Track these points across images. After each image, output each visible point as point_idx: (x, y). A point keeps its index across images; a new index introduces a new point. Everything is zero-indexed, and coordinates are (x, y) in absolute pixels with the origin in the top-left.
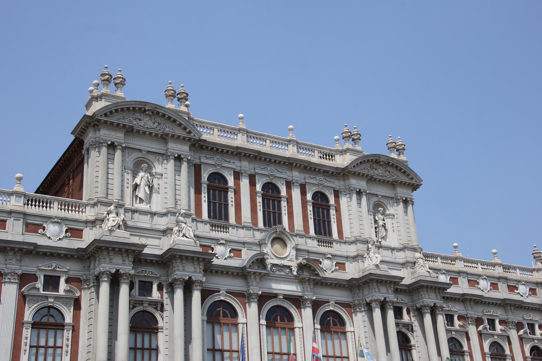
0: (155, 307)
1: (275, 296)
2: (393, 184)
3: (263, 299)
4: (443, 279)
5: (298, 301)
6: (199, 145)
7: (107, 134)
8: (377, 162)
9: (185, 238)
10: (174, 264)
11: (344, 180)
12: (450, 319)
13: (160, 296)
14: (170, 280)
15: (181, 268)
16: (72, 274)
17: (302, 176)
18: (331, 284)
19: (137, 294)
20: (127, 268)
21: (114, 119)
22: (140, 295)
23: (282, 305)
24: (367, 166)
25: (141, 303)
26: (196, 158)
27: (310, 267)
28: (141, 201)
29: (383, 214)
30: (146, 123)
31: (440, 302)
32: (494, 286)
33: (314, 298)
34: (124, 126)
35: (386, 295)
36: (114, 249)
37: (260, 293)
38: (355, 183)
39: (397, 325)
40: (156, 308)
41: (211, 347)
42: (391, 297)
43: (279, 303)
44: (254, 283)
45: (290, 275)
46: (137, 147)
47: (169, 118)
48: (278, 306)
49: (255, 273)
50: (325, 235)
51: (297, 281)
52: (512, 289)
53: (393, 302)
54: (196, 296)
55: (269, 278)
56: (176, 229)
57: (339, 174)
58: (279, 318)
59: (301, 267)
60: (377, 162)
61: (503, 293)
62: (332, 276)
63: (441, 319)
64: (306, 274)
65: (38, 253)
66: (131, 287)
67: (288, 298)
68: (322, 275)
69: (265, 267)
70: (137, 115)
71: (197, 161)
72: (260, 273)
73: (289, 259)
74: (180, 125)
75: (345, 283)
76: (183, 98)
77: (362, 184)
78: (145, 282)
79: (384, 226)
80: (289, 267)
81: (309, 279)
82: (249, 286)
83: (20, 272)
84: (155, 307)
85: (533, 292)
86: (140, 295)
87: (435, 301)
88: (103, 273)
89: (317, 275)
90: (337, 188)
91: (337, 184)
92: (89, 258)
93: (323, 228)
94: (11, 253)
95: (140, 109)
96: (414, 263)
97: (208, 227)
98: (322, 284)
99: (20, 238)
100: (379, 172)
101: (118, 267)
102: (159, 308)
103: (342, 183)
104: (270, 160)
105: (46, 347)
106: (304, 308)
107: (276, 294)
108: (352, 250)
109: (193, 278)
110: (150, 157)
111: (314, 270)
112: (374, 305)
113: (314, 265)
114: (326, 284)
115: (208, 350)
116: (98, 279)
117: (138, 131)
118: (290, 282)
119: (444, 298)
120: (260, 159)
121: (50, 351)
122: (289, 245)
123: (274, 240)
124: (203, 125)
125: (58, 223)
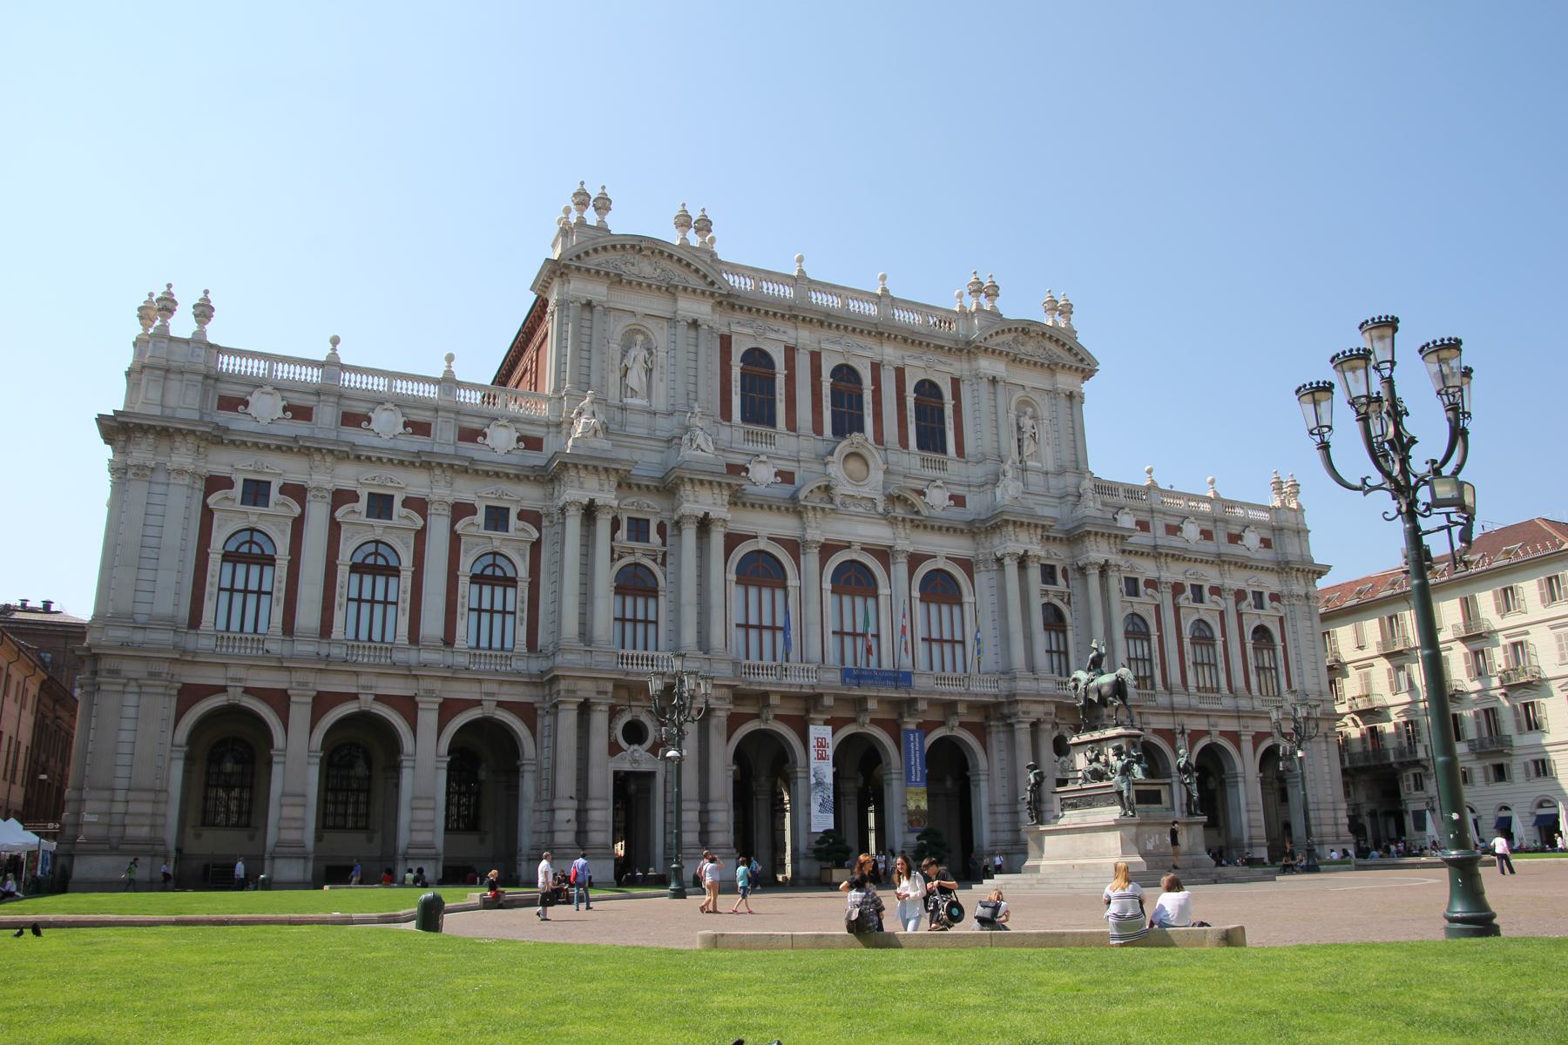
1: (848, 546)
2: (1051, 367)
3: (827, 550)
4: (1127, 521)
5: (884, 555)
6: (730, 302)
7: (580, 288)
8: (1025, 332)
9: (699, 452)
11: (970, 360)
12: (1132, 587)
16: (528, 505)
17: (899, 353)
18: (940, 528)
20: (606, 496)
21: (593, 261)
24: (1008, 337)
25: (632, 552)
27: (906, 500)
28: (634, 393)
29: (1032, 418)
30: (645, 268)
31: (1115, 558)
32: (1207, 535)
34: (607, 274)
35: (1028, 547)
36: (586, 467)
38: (986, 365)
39: (1045, 593)
40: (655, 560)
41: (742, 621)
42: (1036, 549)
43: (855, 556)
46: (627, 308)
47: (680, 260)
48: (853, 561)
49: (814, 508)
50: (935, 451)
52: (1234, 539)
53: (1039, 558)
54: (717, 540)
56: (686, 438)
57: (961, 350)
59: (893, 499)
60: (1025, 332)
61: (1220, 544)
62: (944, 514)
63: (1116, 584)
64: (899, 511)
65: (476, 471)
67: (867, 549)
68: (925, 512)
69: (831, 501)
70: (629, 257)
71: (725, 331)
72: (823, 509)
74: (697, 271)
77: (997, 367)
78: (637, 520)
79: (1033, 437)
80: (872, 500)
81: (904, 520)
82: (805, 529)
83: (450, 500)
85: (1266, 543)
87: (1108, 556)
88: (570, 504)
89: (917, 513)
90: (957, 375)
91: (959, 367)
92: (552, 480)
93: (931, 439)
94: (438, 472)
95: (633, 247)
96: (1080, 496)
97: (739, 435)
98: (925, 527)
99: (450, 450)
100: (1030, 347)
103: (965, 365)
104: (846, 328)
108: (978, 473)
110: (650, 324)
111: (913, 505)
112: (1007, 561)
113: (914, 498)
114: (933, 527)
115: (738, 625)
116: (563, 510)
117: (630, 282)
119: (1124, 552)
120: (830, 325)
122: (872, 465)
123: (848, 456)
124: (736, 269)
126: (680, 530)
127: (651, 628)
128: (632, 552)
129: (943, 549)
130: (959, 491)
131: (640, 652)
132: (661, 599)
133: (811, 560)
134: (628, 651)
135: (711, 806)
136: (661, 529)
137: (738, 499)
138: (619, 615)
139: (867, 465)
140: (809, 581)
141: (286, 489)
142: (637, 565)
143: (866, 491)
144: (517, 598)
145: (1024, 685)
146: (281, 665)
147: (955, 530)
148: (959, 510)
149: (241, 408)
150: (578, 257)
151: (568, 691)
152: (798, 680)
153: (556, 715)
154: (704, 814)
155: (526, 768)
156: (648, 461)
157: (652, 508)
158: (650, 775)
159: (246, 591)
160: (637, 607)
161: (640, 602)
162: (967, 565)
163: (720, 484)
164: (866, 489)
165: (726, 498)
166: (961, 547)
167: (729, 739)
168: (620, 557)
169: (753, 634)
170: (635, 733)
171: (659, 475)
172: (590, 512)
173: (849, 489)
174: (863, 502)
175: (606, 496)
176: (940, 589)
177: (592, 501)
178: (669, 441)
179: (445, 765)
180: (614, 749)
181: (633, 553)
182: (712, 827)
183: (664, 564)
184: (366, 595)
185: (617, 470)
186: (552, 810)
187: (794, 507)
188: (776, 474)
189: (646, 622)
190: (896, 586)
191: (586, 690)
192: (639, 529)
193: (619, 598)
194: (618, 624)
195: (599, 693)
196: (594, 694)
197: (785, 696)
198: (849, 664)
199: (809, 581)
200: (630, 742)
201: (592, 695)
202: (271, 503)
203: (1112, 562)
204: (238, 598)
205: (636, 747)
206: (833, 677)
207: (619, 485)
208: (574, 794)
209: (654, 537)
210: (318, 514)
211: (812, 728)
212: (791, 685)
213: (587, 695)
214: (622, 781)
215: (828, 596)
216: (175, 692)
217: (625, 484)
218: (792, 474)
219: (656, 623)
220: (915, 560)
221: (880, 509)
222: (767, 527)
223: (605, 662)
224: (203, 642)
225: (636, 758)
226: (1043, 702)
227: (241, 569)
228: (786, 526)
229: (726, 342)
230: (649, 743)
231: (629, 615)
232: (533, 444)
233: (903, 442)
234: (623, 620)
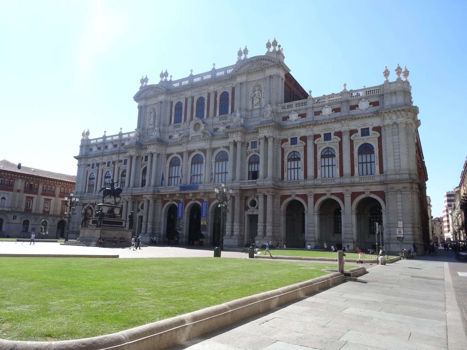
3: (190, 153)
26: (169, 98)
76: (166, 74)
124: (175, 82)
141: (374, 129)
144: (336, 160)
146: (304, 187)
149: (357, 108)
150: (138, 97)
159: (294, 169)
167: (163, 207)
190: (209, 159)
202: (370, 134)
206: (178, 188)
210: (346, 138)
216: (279, 198)
220: (213, 150)
224: (85, 195)
229: (172, 103)
233: (215, 115)
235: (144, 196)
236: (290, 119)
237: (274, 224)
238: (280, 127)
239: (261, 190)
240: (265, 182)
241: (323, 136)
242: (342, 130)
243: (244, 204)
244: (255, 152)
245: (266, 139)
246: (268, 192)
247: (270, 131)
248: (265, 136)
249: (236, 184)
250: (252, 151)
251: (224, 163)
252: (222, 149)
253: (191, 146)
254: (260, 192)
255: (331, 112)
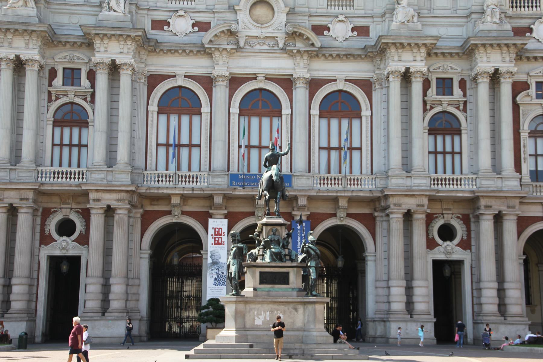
0: (83, 97)
3: (235, 82)
10: (477, 55)
13: (462, 93)
14: (473, 74)
15: (102, 49)
18: (338, 56)
19: (435, 92)
22: (437, 94)
23: (265, 87)
33: (307, 76)
37: (227, 74)
43: (261, 85)
44: (221, 63)
45: (275, 48)
48: (261, 90)
51: (285, 55)
55: (244, 54)
58: (260, 103)
62: (345, 44)
66: (426, 84)
73: (274, 26)
75: (360, 53)
84: (83, 97)
86: (437, 94)
87: (497, 65)
89: (313, 44)
101: (408, 65)
102: (89, 99)
105: (444, 153)
106: (215, 87)
107: (255, 74)
109: (117, 60)
118: (276, 57)
121: (75, 150)
122: (276, 9)
125: (343, 21)
126: (477, 84)
127: (457, 157)
128: (440, 103)
129: (340, 73)
130: (361, 22)
131: (449, 175)
132: (464, 136)
133: (220, 91)
134: (440, 175)
135: (506, 285)
136: (462, 84)
137: (522, 55)
138: (432, 149)
139: (273, 9)
140: (221, 106)
142: (444, 112)
143: (269, 32)
145: (397, 182)
147: (353, 56)
148: (363, 38)
151: (395, 205)
152: (204, 184)
153: (388, 221)
154: (501, 291)
155: (369, 258)
156: (450, 33)
157: (453, 69)
158: (460, 263)
160: (446, 142)
161: (76, 131)
162: (367, 86)
163: (507, 45)
164: (270, 30)
165: (514, 56)
166: (361, 70)
168: (432, 108)
169: (440, 157)
170: (447, 233)
171: (460, 44)
172: (406, 77)
173: (255, 31)
174: (268, 41)
175: (417, 63)
176: (340, 106)
177: (408, 69)
178: (468, 17)
179: (147, 256)
180: (431, 244)
181: (441, 104)
182: (507, 301)
183: (465, 110)
184: (66, 141)
185: (425, 45)
186: (389, 288)
187: (204, 51)
188: (193, 25)
189: (453, 153)
190: (298, 106)
191: (410, 203)
192: (445, 86)
193: (432, 138)
194: (432, 156)
195: (21, 199)
196: (17, 201)
197: (351, 200)
198: (234, 169)
199: (221, 106)
200: (444, 239)
201: (16, 203)
203: (502, 70)
204: (66, 150)
205: (448, 243)
207: (429, 55)
208: (100, 274)
209: (457, 92)
211: (210, 220)
212: (184, 189)
213: (11, 201)
214: (438, 265)
215: (315, 120)
217: (432, 52)
218: (367, 28)
219: (460, 153)
220: (314, 85)
221: (281, 45)
222: (181, 68)
223: (421, 183)
225: (64, 246)
226: (413, 196)
227: (67, 131)
228: (200, 66)
230: (457, 241)
231: (440, 149)
232: (362, 31)
234: (436, 153)
235: (92, 196)
236: (534, 35)
237: (129, 279)
238: (147, 45)
239: (493, 202)
240: (14, 175)
241: (533, 86)
242: (215, 73)
243: (38, 228)
244: (76, 96)
245: (114, 69)
246: (509, 207)
247: (125, 50)
248: (113, 61)
249: (417, 181)
250: (71, 95)
251: (185, 119)
252: (340, 86)
253: (242, 65)
254: (488, 207)
255: (191, 29)
